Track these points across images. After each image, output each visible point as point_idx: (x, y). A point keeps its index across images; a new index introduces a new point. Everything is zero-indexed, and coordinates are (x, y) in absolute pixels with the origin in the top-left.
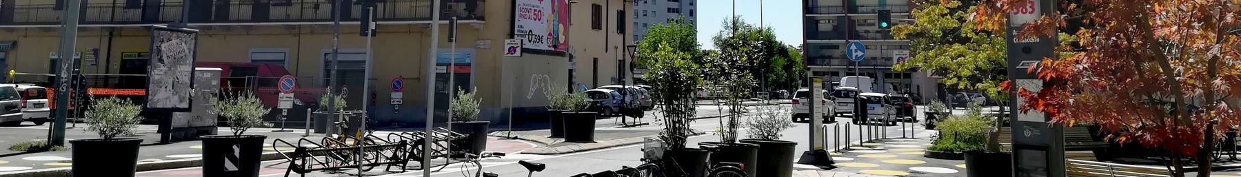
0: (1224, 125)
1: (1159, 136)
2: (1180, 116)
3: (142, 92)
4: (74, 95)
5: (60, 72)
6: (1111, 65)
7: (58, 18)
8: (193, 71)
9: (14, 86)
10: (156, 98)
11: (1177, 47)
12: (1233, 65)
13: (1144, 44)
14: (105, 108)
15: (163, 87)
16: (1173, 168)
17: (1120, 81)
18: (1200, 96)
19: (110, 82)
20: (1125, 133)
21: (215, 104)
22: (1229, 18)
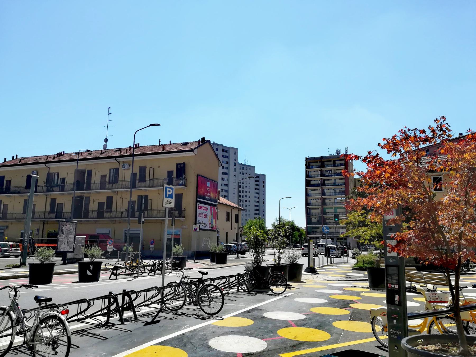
0: (465, 257)
1: (441, 261)
2: (448, 254)
3: (55, 245)
4: (30, 246)
5: (25, 238)
6: (422, 235)
7: (24, 217)
8: (75, 237)
9: (7, 243)
10: (61, 248)
11: (447, 228)
12: (469, 235)
13: (435, 227)
14: (41, 251)
15: (64, 243)
16: (446, 274)
17: (426, 241)
18: (456, 246)
19: (44, 241)
20: (428, 260)
21: (83, 249)
22: (467, 217)
